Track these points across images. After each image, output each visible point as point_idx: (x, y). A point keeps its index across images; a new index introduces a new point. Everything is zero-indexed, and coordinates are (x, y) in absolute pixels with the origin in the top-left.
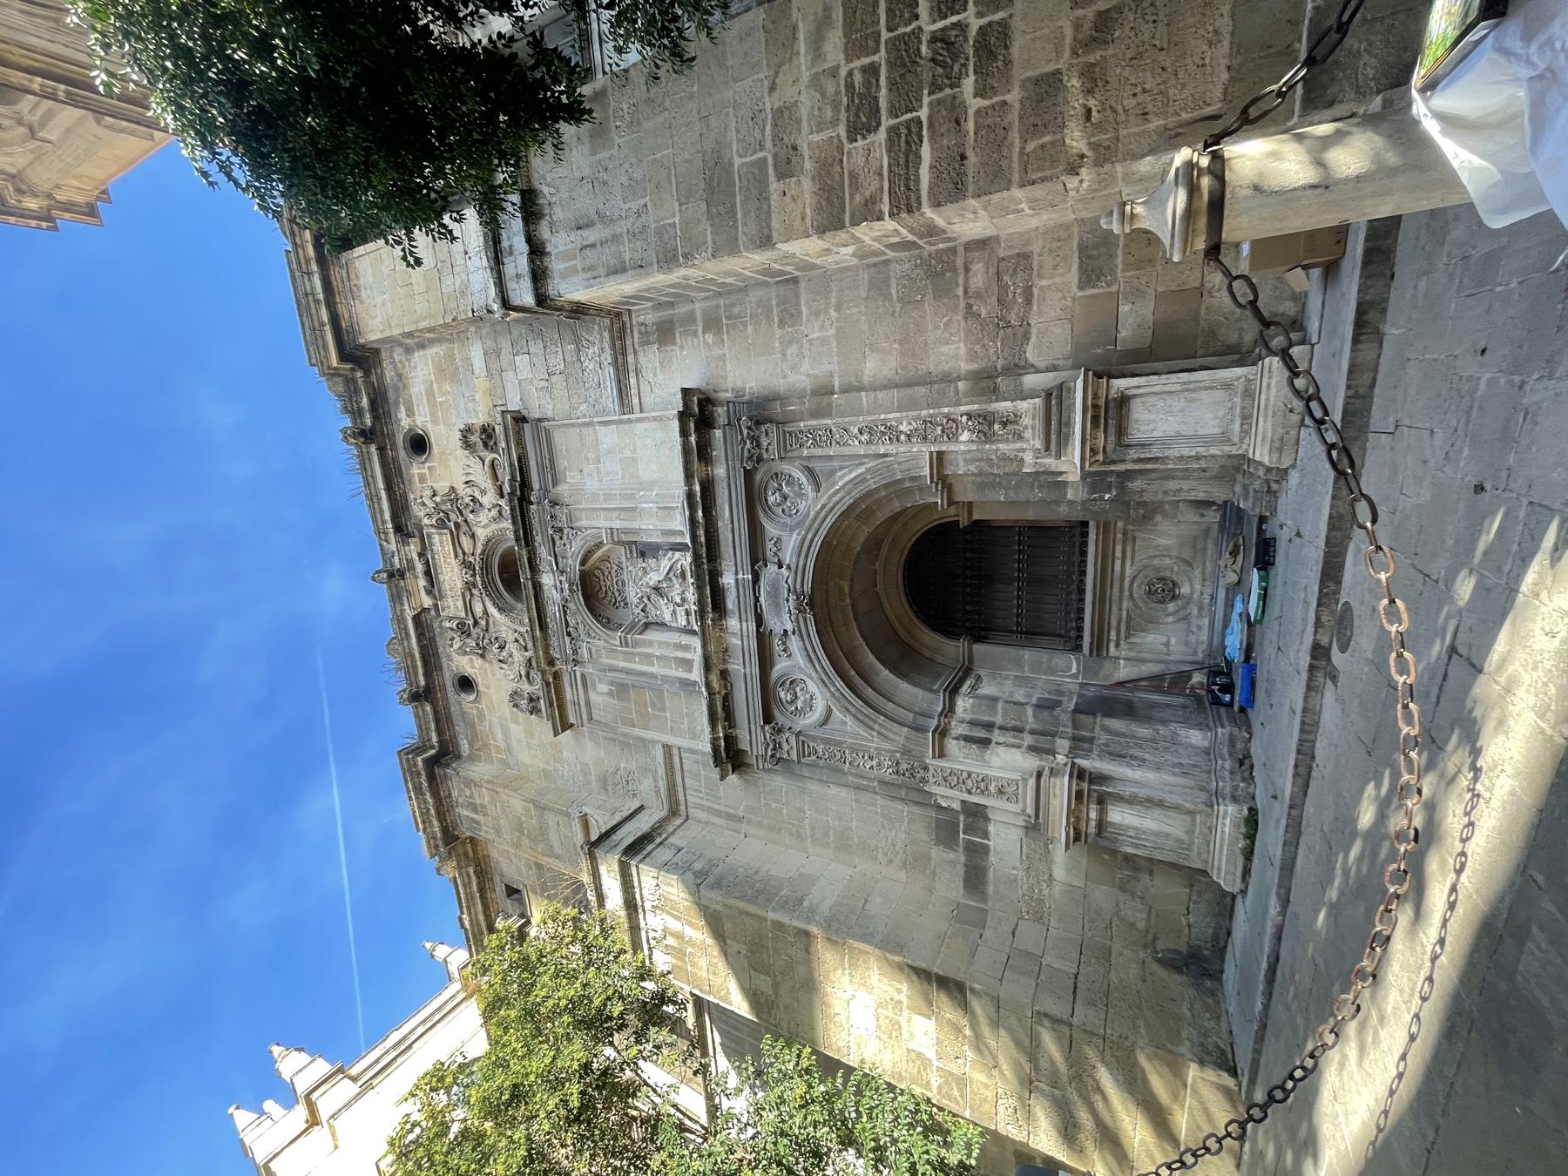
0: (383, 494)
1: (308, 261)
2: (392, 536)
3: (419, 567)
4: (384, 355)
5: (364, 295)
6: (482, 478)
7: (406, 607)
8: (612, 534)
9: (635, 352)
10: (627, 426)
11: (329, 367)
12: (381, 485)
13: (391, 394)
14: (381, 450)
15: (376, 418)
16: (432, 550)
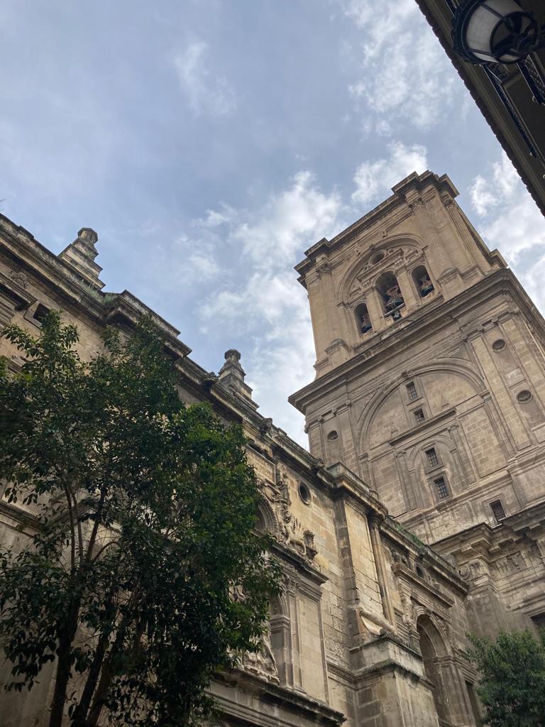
0: (293, 455)
1: (371, 502)
2: (277, 442)
3: (263, 447)
4: (332, 502)
5: (356, 518)
6: (298, 535)
7: (248, 420)
8: (286, 624)
9: (344, 685)
10: (321, 662)
11: (343, 479)
12: (297, 458)
13: (320, 493)
14: (306, 469)
15: (317, 477)
16: (266, 461)
